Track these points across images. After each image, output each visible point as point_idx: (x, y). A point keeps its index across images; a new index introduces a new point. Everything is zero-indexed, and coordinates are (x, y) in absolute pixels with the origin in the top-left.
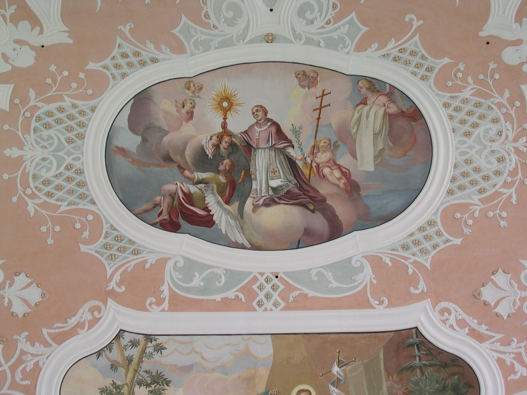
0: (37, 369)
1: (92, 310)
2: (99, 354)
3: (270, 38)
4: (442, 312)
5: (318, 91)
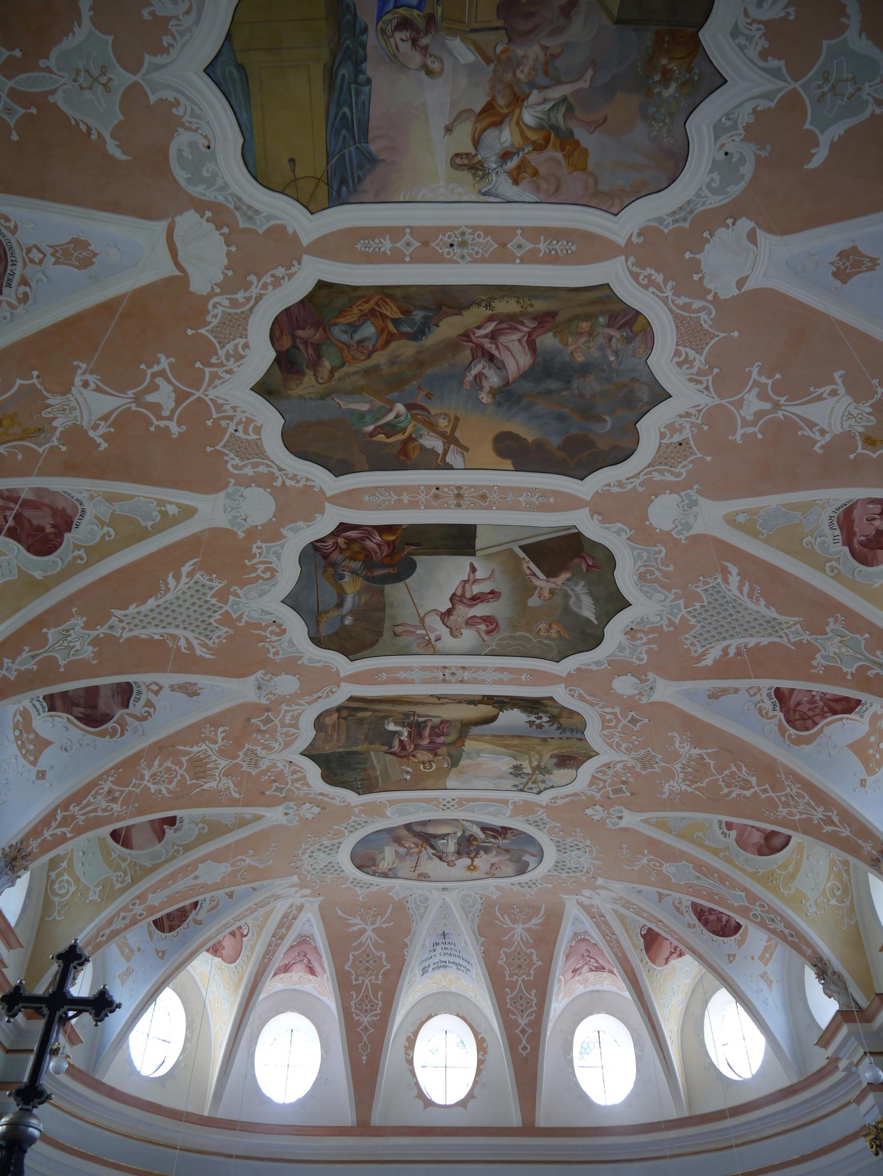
0: (591, 784)
1: (556, 802)
2: (552, 787)
3: (445, 889)
4: (344, 801)
5: (417, 872)
